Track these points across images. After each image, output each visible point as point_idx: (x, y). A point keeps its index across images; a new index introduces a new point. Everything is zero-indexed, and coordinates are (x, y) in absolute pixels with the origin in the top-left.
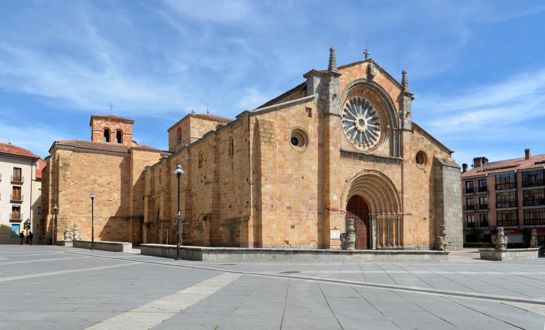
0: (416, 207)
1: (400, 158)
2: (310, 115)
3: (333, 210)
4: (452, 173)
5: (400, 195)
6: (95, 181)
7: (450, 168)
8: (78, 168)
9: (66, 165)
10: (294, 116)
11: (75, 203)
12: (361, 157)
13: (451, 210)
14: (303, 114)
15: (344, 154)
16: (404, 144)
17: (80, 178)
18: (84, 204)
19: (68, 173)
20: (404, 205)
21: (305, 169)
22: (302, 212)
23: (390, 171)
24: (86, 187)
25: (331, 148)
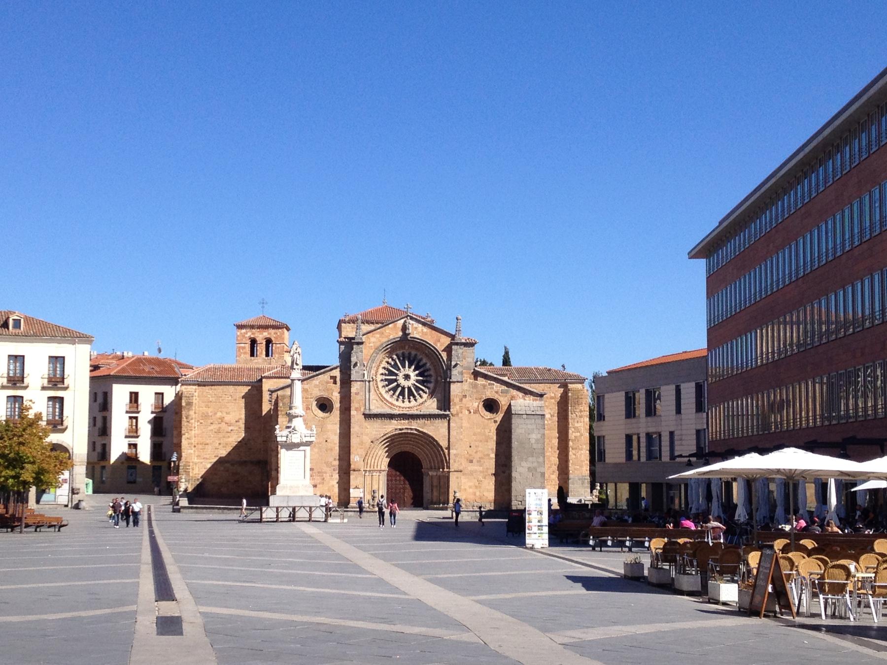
0: (478, 461)
1: (447, 413)
2: (335, 383)
3: (354, 470)
4: (528, 421)
5: (446, 451)
6: (222, 419)
7: (525, 416)
8: (203, 405)
9: (189, 404)
10: (316, 386)
11: (200, 446)
12: (391, 417)
13: (524, 464)
14: (328, 383)
15: (368, 416)
16: (452, 398)
17: (205, 416)
18: (210, 447)
19: (192, 413)
20: (451, 461)
21: (329, 433)
22: (326, 473)
23: (432, 427)
24: (212, 427)
25: (353, 412)
